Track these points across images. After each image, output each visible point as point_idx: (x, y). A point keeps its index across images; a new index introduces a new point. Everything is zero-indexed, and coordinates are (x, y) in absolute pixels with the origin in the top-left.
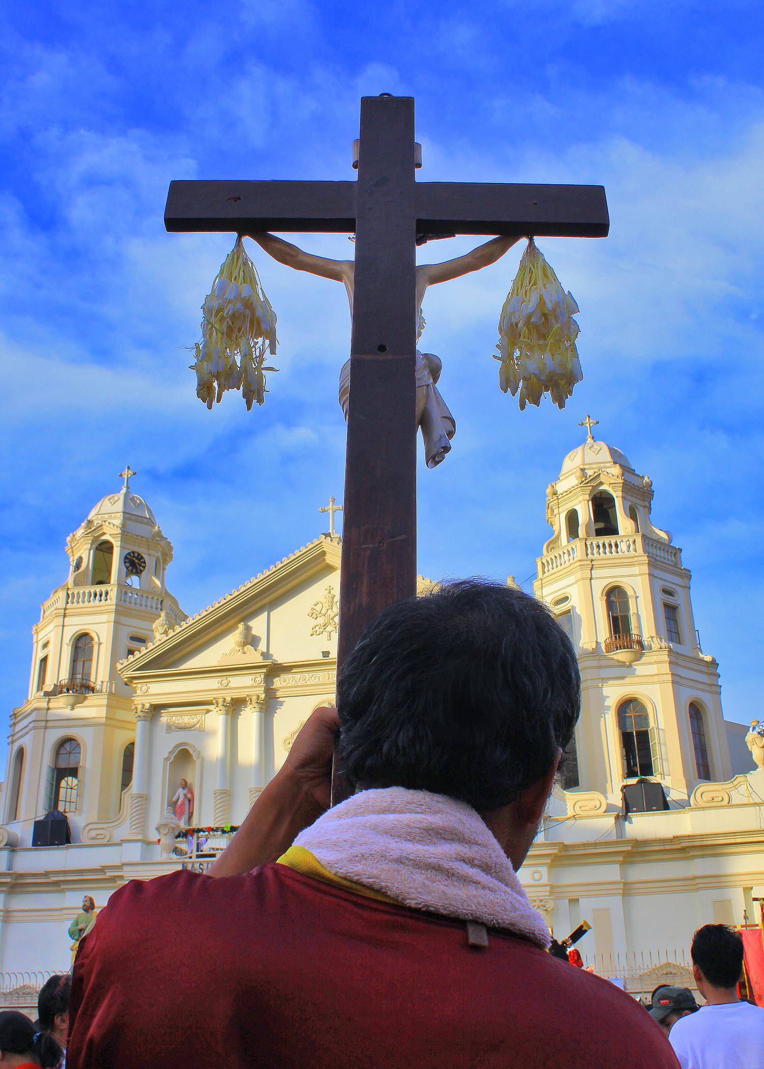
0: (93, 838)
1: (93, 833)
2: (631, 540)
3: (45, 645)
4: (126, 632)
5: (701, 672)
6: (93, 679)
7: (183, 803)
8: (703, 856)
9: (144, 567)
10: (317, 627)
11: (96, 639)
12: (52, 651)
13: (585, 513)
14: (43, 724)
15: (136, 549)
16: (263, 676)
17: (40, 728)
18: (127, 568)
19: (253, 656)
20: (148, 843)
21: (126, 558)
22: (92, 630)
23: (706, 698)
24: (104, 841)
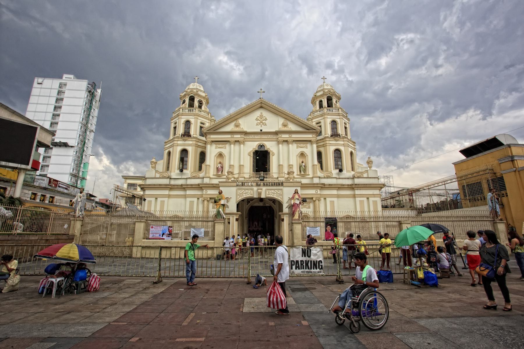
0: (194, 176)
1: (194, 175)
3: (176, 123)
4: (199, 121)
6: (190, 133)
7: (220, 168)
8: (360, 189)
14: (177, 145)
15: (201, 99)
17: (176, 146)
23: (353, 151)
24: (198, 177)
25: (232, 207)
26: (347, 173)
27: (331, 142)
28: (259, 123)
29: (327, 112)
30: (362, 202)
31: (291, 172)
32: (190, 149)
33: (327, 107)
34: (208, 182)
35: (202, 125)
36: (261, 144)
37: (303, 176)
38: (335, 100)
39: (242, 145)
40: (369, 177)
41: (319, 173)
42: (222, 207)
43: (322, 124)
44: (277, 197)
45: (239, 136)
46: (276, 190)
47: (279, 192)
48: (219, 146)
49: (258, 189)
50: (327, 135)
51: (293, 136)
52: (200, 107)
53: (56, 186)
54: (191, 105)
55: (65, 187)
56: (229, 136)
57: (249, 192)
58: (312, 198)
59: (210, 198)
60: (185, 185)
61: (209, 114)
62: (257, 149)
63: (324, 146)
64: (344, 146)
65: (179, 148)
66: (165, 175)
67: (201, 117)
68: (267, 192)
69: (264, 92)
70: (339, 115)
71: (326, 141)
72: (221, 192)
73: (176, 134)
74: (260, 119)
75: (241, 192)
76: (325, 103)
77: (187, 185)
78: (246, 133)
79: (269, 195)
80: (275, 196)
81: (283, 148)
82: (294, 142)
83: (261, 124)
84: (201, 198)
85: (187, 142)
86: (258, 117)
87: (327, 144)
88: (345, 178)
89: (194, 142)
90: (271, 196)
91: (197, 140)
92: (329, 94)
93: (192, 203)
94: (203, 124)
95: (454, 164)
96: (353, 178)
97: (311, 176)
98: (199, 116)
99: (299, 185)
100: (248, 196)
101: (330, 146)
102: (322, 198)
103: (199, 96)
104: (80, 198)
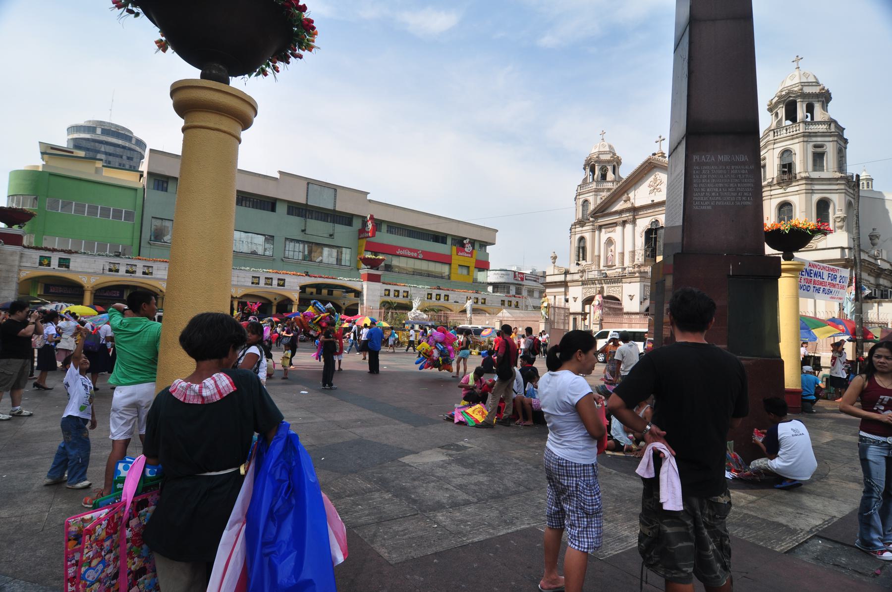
13: (782, 112)
19: (628, 205)
22: (589, 198)
27: (773, 193)
29: (776, 138)
36: (654, 220)
40: (828, 247)
48: (608, 230)
53: (522, 279)
55: (532, 279)
64: (799, 194)
65: (578, 236)
67: (600, 191)
69: (664, 140)
78: (635, 210)
83: (655, 191)
89: (591, 227)
101: (771, 199)
103: (599, 161)
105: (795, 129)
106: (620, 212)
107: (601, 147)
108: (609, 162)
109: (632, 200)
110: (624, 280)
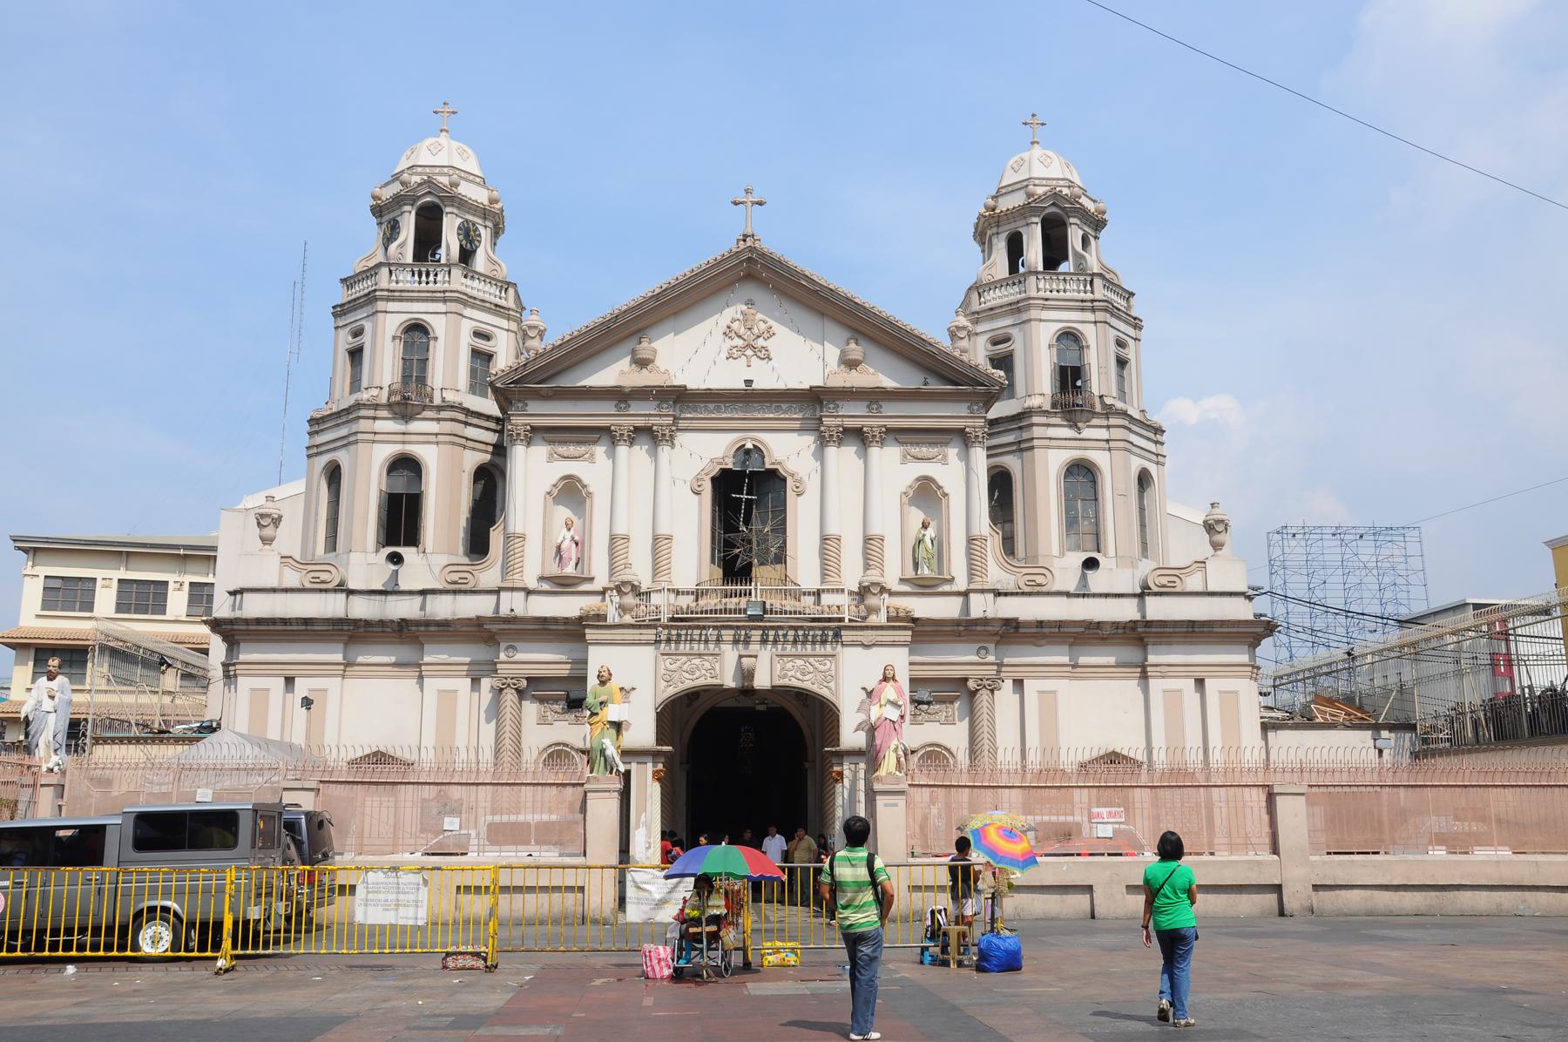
0: (455, 583)
2: (1089, 279)
3: (358, 333)
4: (467, 327)
5: (1148, 439)
7: (570, 548)
9: (480, 242)
10: (735, 350)
11: (432, 335)
12: (366, 339)
16: (671, 402)
17: (367, 441)
18: (461, 241)
20: (529, 592)
21: (459, 228)
23: (1153, 468)
25: (643, 732)
26: (1114, 575)
27: (1051, 432)
28: (742, 350)
30: (1173, 696)
31: (873, 584)
32: (428, 455)
33: (1041, 268)
34: (519, 612)
35: (482, 344)
36: (749, 446)
37: (925, 587)
38: (1081, 233)
39: (664, 451)
40: (1211, 588)
41: (996, 573)
42: (613, 732)
43: (1017, 346)
44: (815, 688)
45: (648, 408)
46: (811, 660)
47: (822, 668)
49: (741, 657)
50: (1035, 402)
51: (890, 409)
52: (466, 256)
54: (427, 242)
56: (609, 407)
57: (707, 665)
58: (966, 680)
59: (527, 679)
60: (418, 623)
61: (511, 291)
62: (730, 466)
63: (1022, 448)
64: (1110, 449)
65: (384, 453)
66: (324, 576)
67: (473, 306)
68: (779, 667)
70: (1093, 310)
71: (1033, 425)
72: (606, 674)
73: (365, 383)
74: (742, 331)
75: (673, 667)
76: (1034, 252)
77: (427, 623)
78: (679, 397)
79: (785, 676)
80: (809, 684)
81: (843, 457)
82: (891, 438)
83: (749, 352)
84: (488, 676)
85: (416, 426)
86: (732, 322)
87: (1036, 443)
88: (1107, 596)
90: (794, 683)
91: (461, 417)
92: (1053, 204)
93: (448, 696)
94: (486, 337)
95: (1549, 543)
96: (1144, 593)
97: (961, 584)
98: (465, 303)
99: (902, 639)
100: (701, 682)
101: (1048, 447)
102: (1008, 677)
103: (462, 204)
104: (52, 697)
105: (1061, 287)
106: (619, 395)
107: (455, 155)
108: (485, 213)
109: (661, 362)
110: (847, 636)
